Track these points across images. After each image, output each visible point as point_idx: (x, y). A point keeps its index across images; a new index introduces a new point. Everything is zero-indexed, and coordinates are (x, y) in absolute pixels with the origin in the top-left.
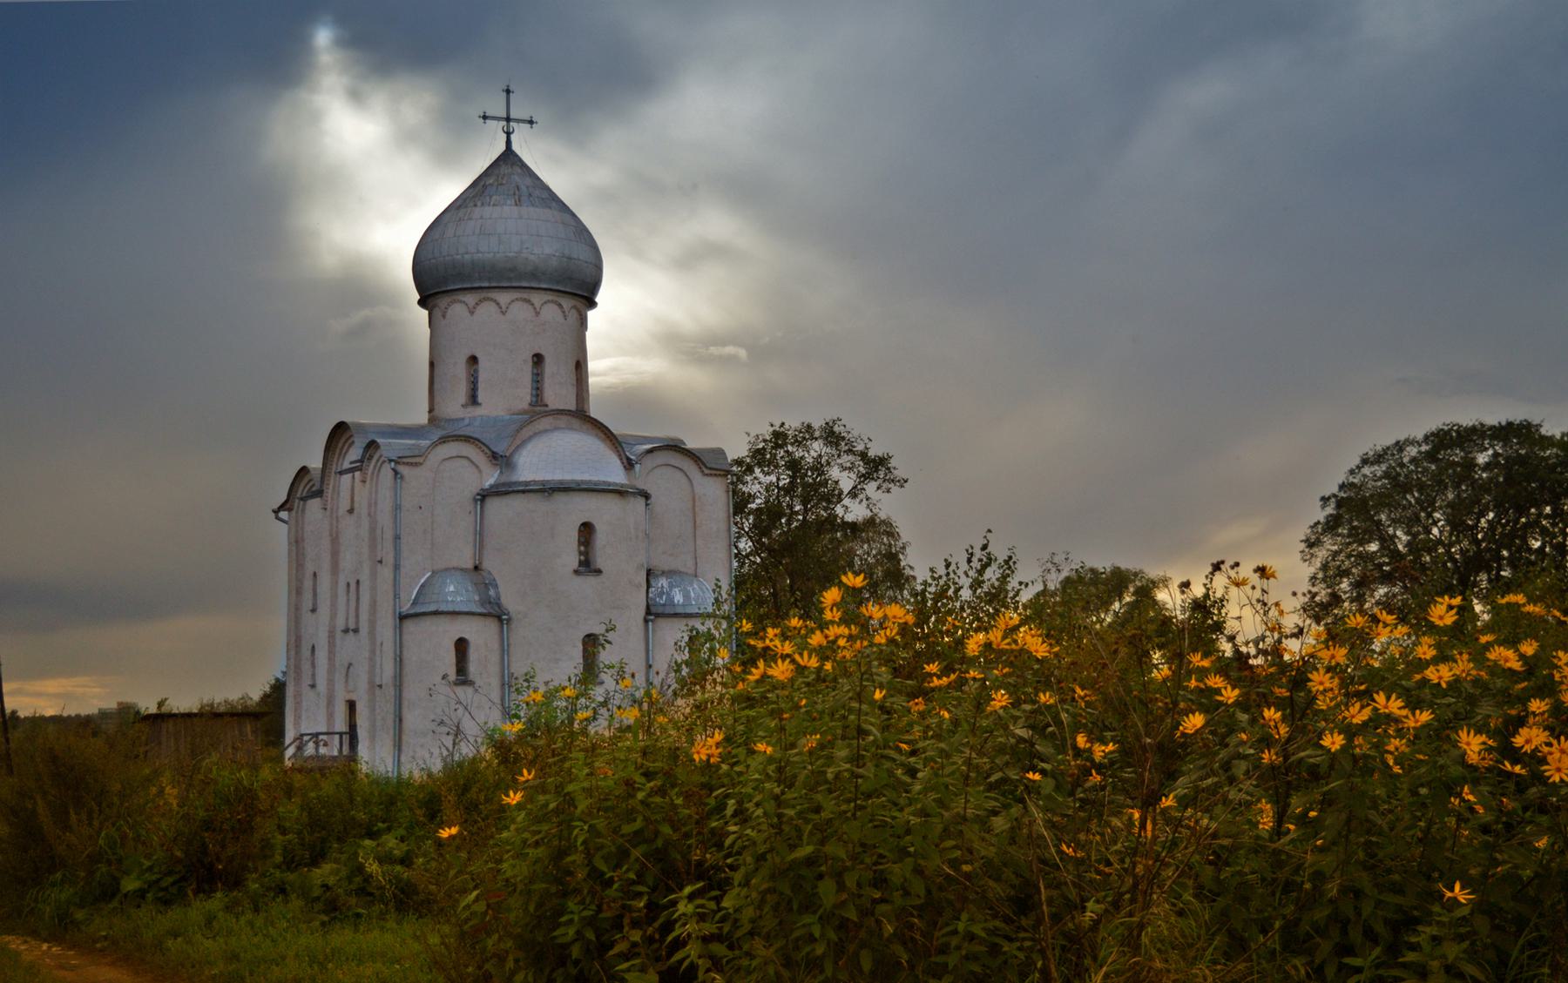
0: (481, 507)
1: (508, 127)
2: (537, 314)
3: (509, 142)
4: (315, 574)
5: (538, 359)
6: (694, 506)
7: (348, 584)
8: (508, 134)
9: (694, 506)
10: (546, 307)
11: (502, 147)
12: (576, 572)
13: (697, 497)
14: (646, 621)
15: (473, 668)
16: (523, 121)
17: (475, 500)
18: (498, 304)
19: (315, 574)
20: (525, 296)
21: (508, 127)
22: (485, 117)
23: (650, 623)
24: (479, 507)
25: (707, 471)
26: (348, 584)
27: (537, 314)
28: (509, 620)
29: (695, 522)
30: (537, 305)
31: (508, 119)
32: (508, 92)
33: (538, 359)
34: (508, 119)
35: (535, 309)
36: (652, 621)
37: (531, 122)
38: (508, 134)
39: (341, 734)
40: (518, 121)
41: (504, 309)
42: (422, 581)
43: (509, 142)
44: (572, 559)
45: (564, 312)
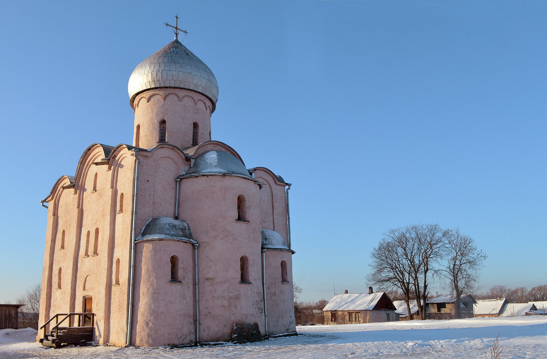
0: (179, 186)
1: (176, 31)
2: (196, 104)
4: (64, 232)
5: (195, 125)
6: (272, 199)
7: (89, 232)
9: (272, 199)
10: (199, 102)
12: (237, 220)
13: (273, 195)
14: (262, 252)
15: (180, 273)
16: (183, 31)
17: (176, 181)
18: (178, 96)
19: (64, 232)
21: (176, 31)
22: (167, 25)
23: (264, 253)
24: (178, 185)
25: (278, 183)
26: (89, 232)
27: (196, 104)
28: (198, 247)
29: (273, 206)
30: (196, 100)
31: (176, 28)
32: (177, 18)
33: (195, 125)
34: (176, 28)
35: (195, 102)
36: (265, 252)
37: (185, 32)
39: (80, 315)
40: (181, 30)
41: (181, 99)
42: (147, 223)
44: (235, 214)
45: (206, 107)
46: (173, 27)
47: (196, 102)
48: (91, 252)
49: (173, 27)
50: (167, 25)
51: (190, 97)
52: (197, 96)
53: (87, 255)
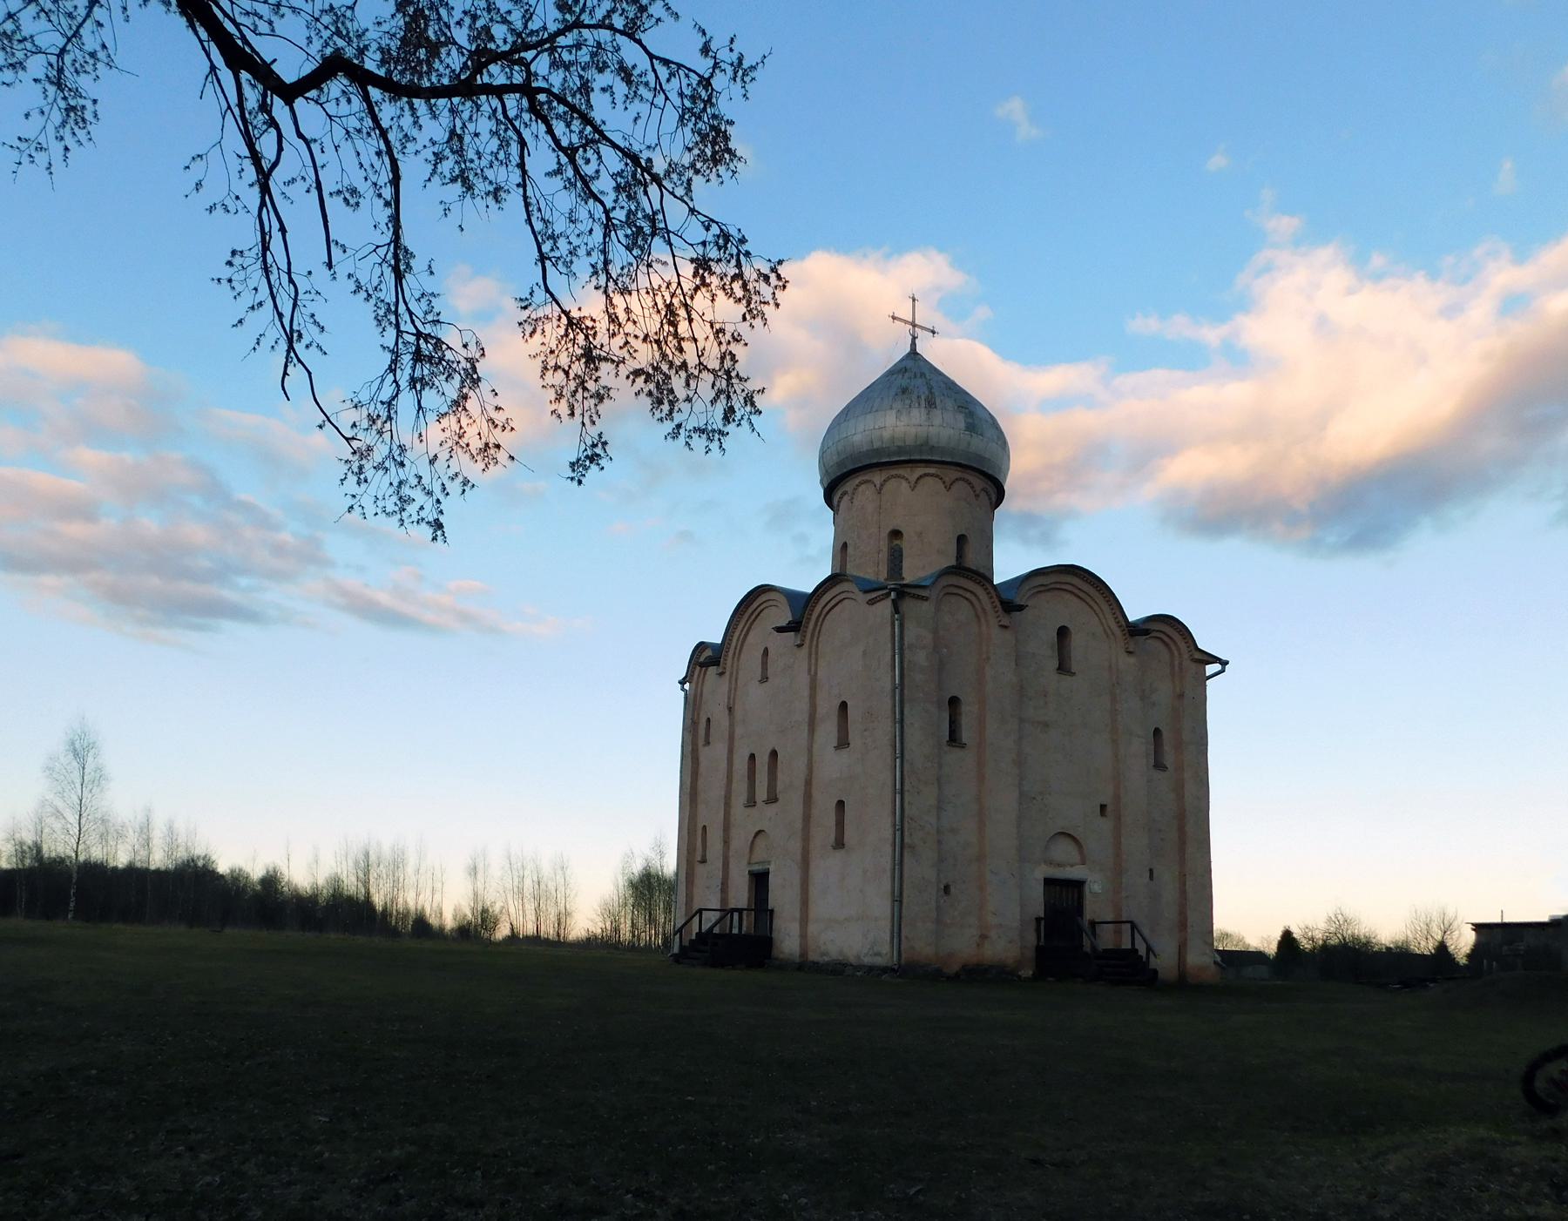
1: (914, 331)
3: (913, 344)
7: (752, 757)
8: (914, 338)
11: (908, 350)
20: (967, 476)
26: (752, 757)
30: (978, 489)
31: (914, 325)
32: (914, 300)
34: (914, 325)
37: (933, 332)
38: (914, 338)
43: (913, 344)
46: (906, 322)
47: (977, 492)
48: (761, 793)
49: (906, 322)
50: (894, 318)
51: (963, 480)
52: (979, 483)
53: (751, 803)
